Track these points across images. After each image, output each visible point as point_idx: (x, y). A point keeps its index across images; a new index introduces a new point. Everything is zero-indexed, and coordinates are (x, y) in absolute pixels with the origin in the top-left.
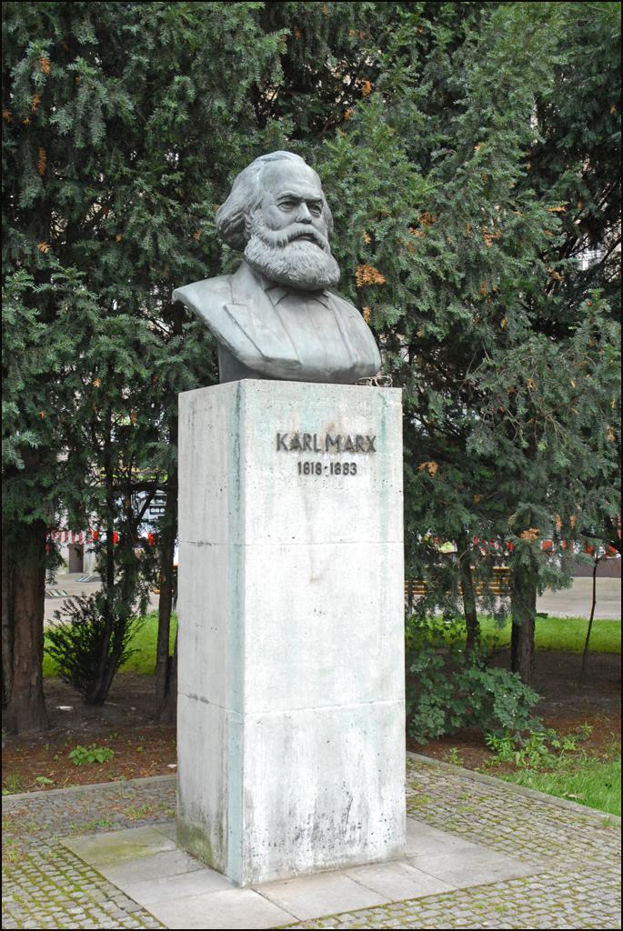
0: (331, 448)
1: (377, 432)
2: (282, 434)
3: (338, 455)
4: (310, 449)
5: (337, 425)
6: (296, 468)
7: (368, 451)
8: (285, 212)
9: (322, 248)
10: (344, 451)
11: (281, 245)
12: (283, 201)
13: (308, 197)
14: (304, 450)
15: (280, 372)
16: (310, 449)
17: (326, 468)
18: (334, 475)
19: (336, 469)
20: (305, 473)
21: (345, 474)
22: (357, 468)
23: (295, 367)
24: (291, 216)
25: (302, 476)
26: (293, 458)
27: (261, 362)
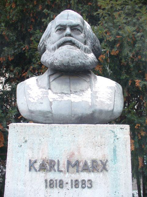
0: (71, 169)
1: (110, 157)
2: (33, 160)
3: (77, 174)
4: (55, 171)
5: (76, 153)
6: (44, 185)
7: (102, 171)
9: (79, 48)
10: (82, 171)
11: (54, 49)
12: (57, 29)
13: (70, 24)
14: (50, 171)
15: (41, 119)
16: (55, 171)
17: (67, 183)
18: (74, 189)
19: (76, 184)
20: (51, 187)
21: (83, 188)
23: (48, 115)
24: (61, 35)
25: (49, 190)
26: (41, 177)
27: (28, 114)
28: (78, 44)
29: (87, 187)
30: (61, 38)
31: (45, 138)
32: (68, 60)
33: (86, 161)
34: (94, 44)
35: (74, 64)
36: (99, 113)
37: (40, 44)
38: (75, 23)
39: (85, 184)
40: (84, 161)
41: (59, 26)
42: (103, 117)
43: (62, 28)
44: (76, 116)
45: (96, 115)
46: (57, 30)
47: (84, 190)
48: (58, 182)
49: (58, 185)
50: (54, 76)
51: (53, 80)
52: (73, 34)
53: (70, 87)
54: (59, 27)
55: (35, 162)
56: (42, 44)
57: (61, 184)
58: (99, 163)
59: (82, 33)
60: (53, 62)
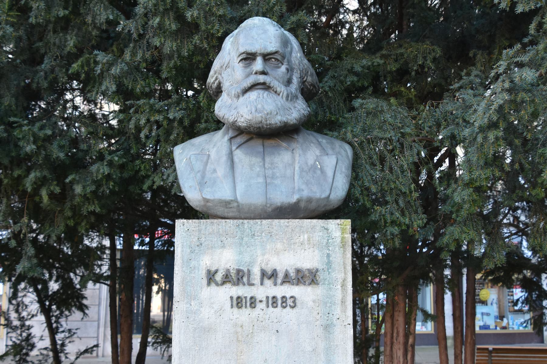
2: (213, 269)
7: (310, 284)
8: (243, 67)
14: (238, 284)
15: (220, 211)
16: (244, 285)
17: (261, 301)
18: (271, 309)
19: (273, 301)
22: (297, 301)
23: (232, 206)
24: (248, 70)
25: (235, 310)
27: (202, 203)
28: (276, 88)
29: (288, 307)
30: (248, 76)
31: (229, 239)
32: (260, 119)
33: (286, 270)
34: (305, 79)
35: (270, 124)
36: (307, 202)
37: (210, 80)
38: (271, 49)
39: (285, 302)
40: (284, 271)
41: (243, 53)
42: (313, 206)
43: (249, 58)
44: (273, 207)
45: (302, 205)
46: (241, 60)
47: (285, 310)
48: (248, 299)
49: (248, 304)
50: (240, 140)
51: (237, 148)
52: (268, 70)
53: (264, 159)
54: (244, 56)
55: (216, 271)
56: (214, 79)
57: (253, 302)
58: (306, 273)
59: (283, 64)
60: (236, 121)
